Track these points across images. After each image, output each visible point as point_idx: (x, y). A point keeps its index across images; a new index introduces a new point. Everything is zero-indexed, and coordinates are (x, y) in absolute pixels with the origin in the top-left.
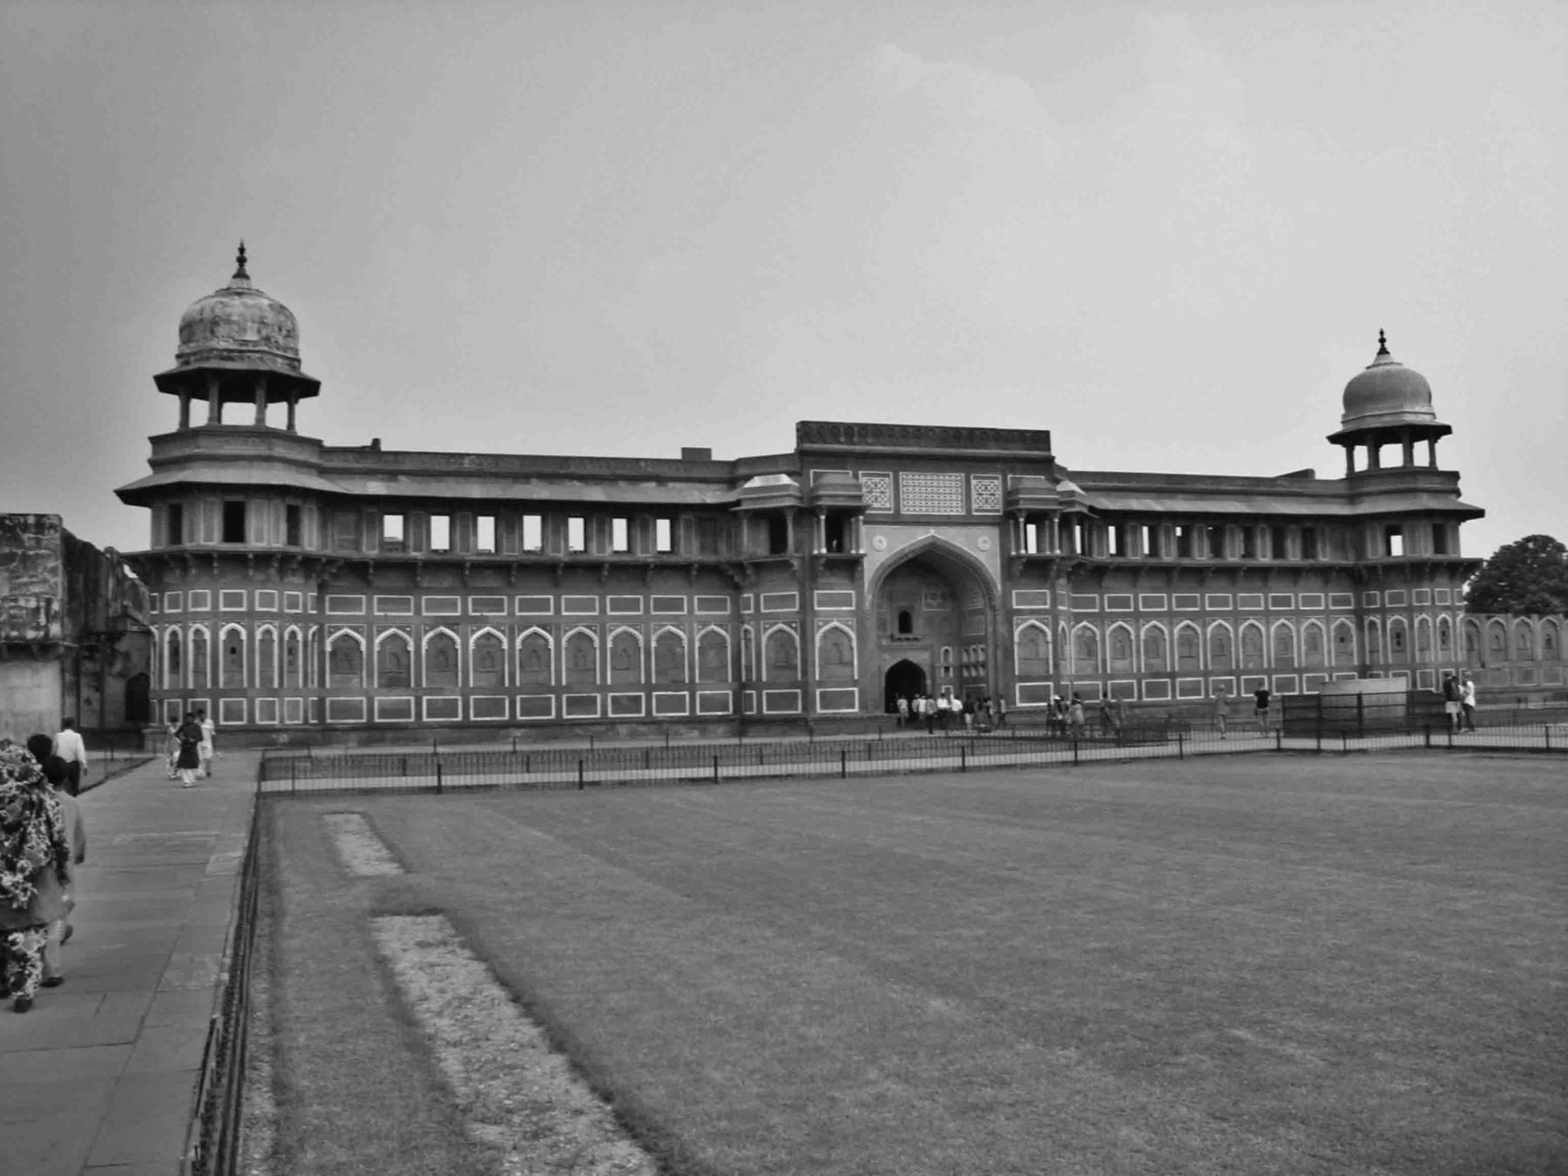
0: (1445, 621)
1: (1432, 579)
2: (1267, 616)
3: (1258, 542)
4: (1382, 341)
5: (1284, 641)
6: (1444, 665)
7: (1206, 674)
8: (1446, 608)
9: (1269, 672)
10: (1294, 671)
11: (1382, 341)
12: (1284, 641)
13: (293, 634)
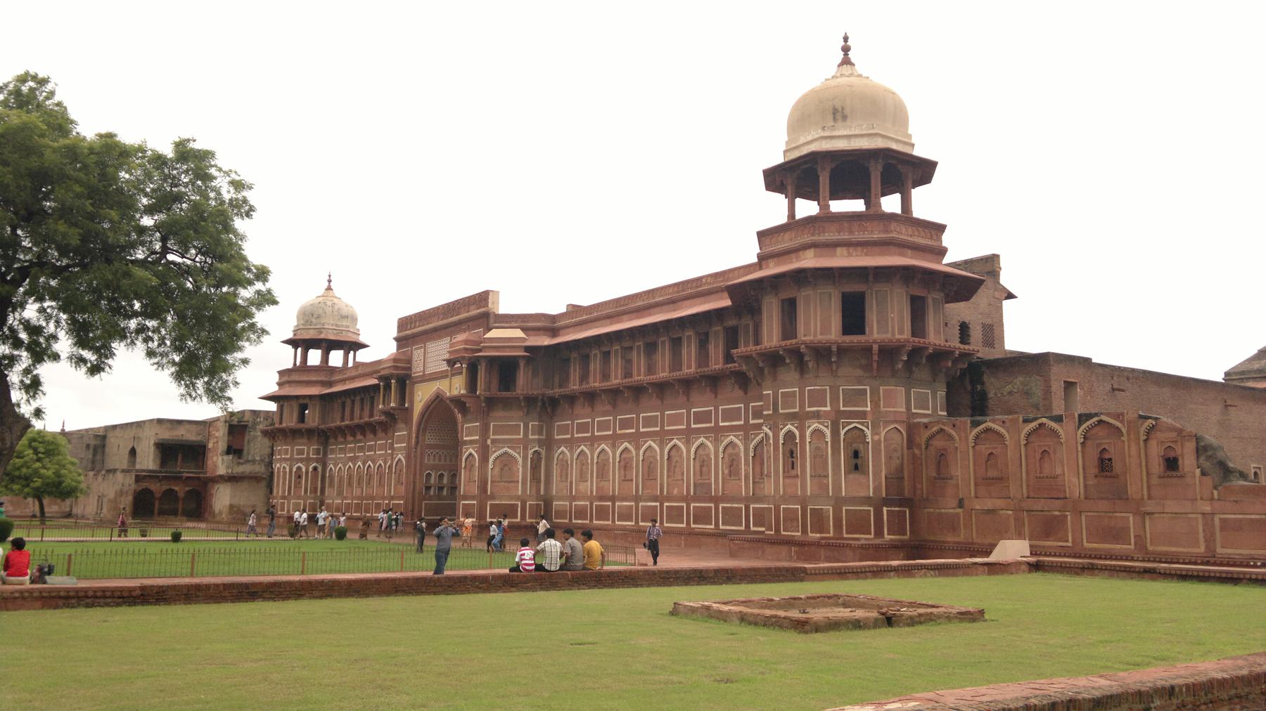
0: (790, 435)
1: (775, 378)
2: (689, 435)
3: (684, 351)
4: (846, 49)
5: (703, 464)
6: (785, 499)
7: (637, 499)
8: (793, 417)
9: (687, 499)
10: (711, 499)
11: (846, 49)
12: (703, 464)
13: (299, 468)
